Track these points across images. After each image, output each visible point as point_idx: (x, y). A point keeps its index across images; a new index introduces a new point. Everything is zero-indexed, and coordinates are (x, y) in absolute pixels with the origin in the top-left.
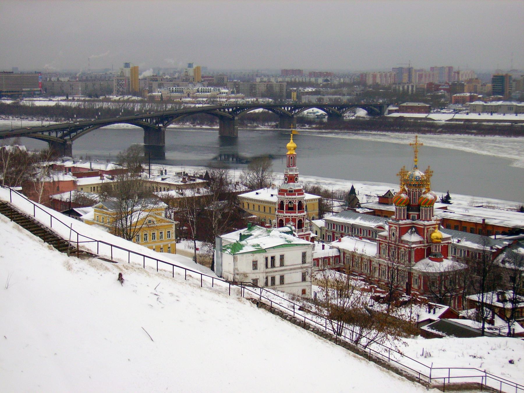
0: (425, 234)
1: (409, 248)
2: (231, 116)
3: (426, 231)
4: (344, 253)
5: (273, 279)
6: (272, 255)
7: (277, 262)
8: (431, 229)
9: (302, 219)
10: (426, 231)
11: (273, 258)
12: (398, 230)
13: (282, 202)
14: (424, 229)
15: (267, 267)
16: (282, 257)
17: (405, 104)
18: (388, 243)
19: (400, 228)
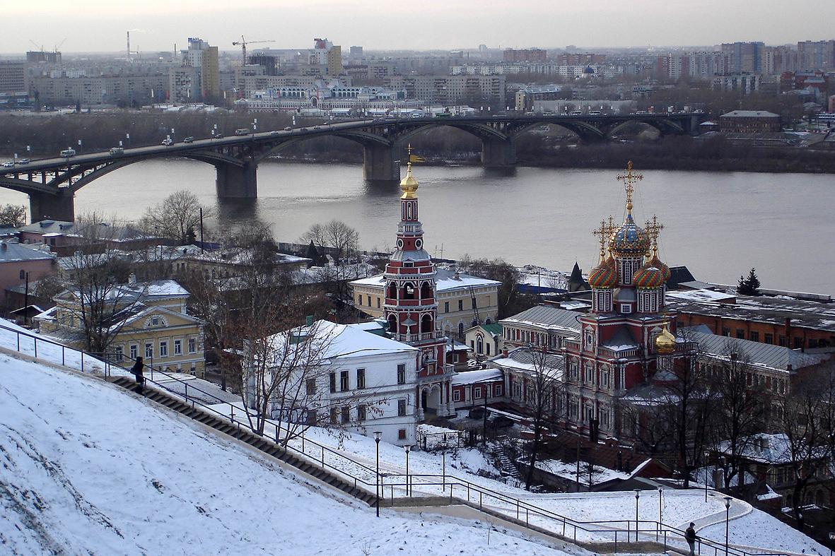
0: (646, 338)
1: (615, 363)
2: (386, 141)
3: (646, 333)
4: (511, 376)
5: (346, 411)
6: (344, 369)
7: (353, 382)
8: (656, 329)
9: (430, 314)
10: (646, 333)
11: (345, 375)
13: (393, 284)
14: (643, 328)
15: (333, 390)
16: (361, 373)
17: (731, 114)
19: (599, 327)
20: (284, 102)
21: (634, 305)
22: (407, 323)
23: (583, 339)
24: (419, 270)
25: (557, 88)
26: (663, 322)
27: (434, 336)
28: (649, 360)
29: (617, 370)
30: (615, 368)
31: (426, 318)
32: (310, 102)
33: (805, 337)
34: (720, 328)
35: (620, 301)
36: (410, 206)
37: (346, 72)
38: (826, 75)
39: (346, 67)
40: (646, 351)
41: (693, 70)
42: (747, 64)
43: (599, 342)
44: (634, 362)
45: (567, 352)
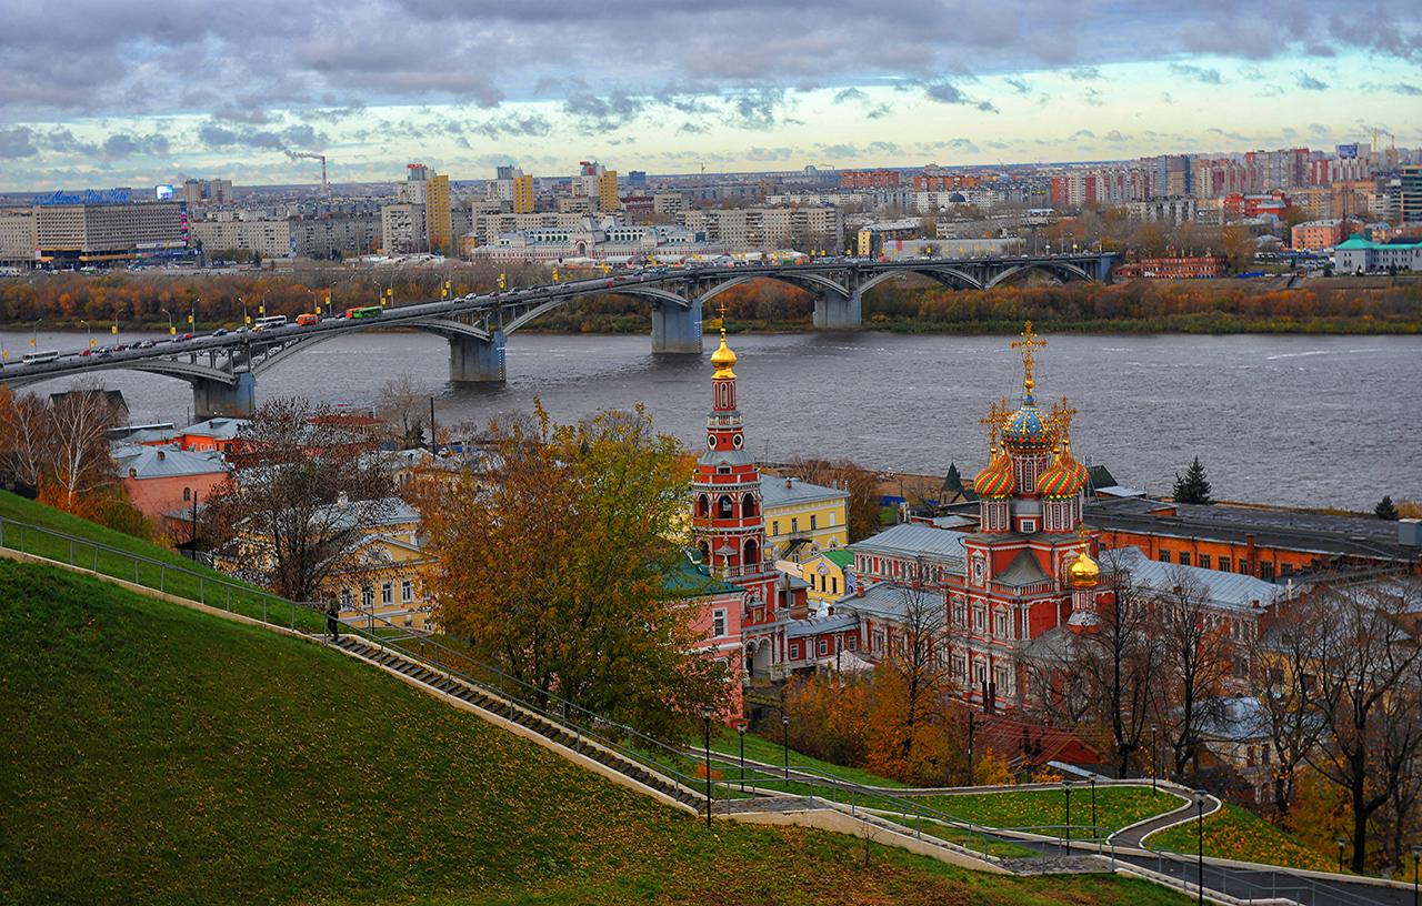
0: (1057, 566)
3: (1057, 560)
9: (755, 538)
10: (1057, 560)
12: (988, 558)
14: (1052, 553)
18: (968, 592)
19: (992, 552)
20: (539, 249)
21: (1040, 521)
22: (724, 550)
23: (969, 570)
24: (739, 477)
25: (913, 222)
26: (1079, 543)
27: (762, 569)
28: (1062, 597)
29: (1018, 612)
30: (1015, 610)
31: (750, 544)
32: (576, 248)
33: (1275, 562)
34: (1155, 550)
35: (1019, 515)
36: (724, 389)
37: (624, 206)
38: (1287, 197)
39: (623, 200)
40: (1057, 585)
41: (1101, 193)
42: (1175, 186)
43: (992, 572)
44: (1042, 601)
45: (947, 587)
